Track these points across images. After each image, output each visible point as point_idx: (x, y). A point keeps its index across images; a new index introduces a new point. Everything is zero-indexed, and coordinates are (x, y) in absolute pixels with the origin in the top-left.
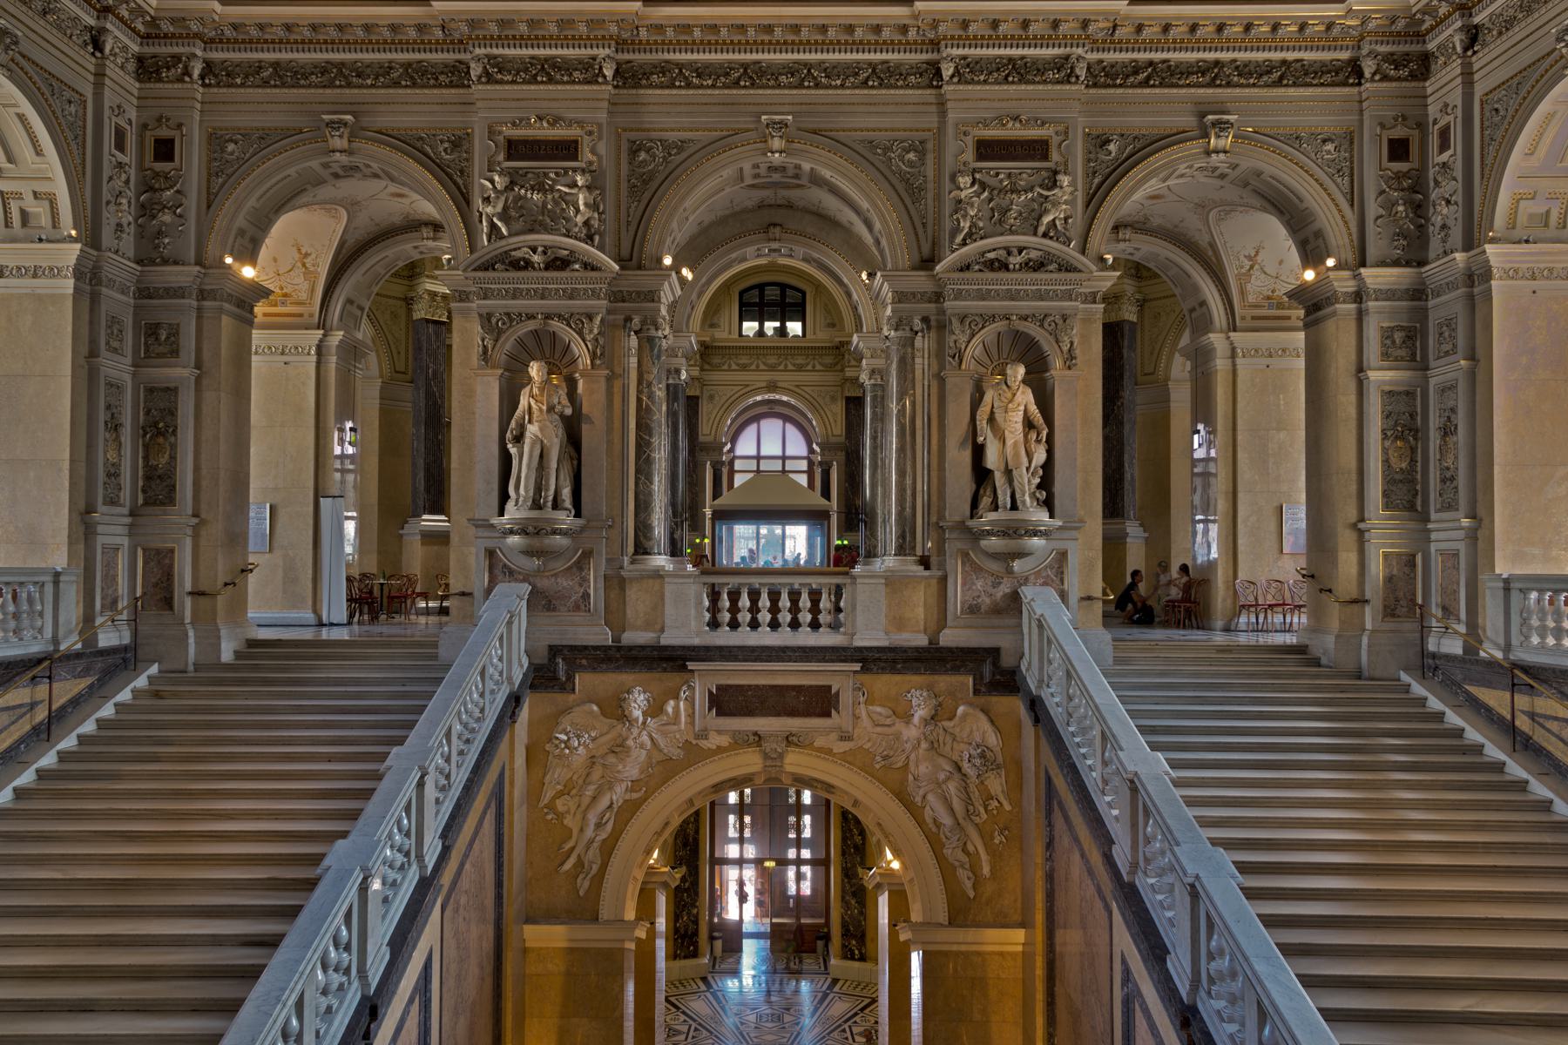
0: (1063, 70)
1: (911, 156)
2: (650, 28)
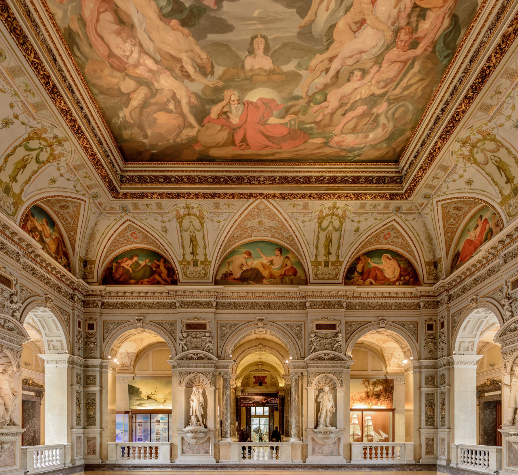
0: (339, 305)
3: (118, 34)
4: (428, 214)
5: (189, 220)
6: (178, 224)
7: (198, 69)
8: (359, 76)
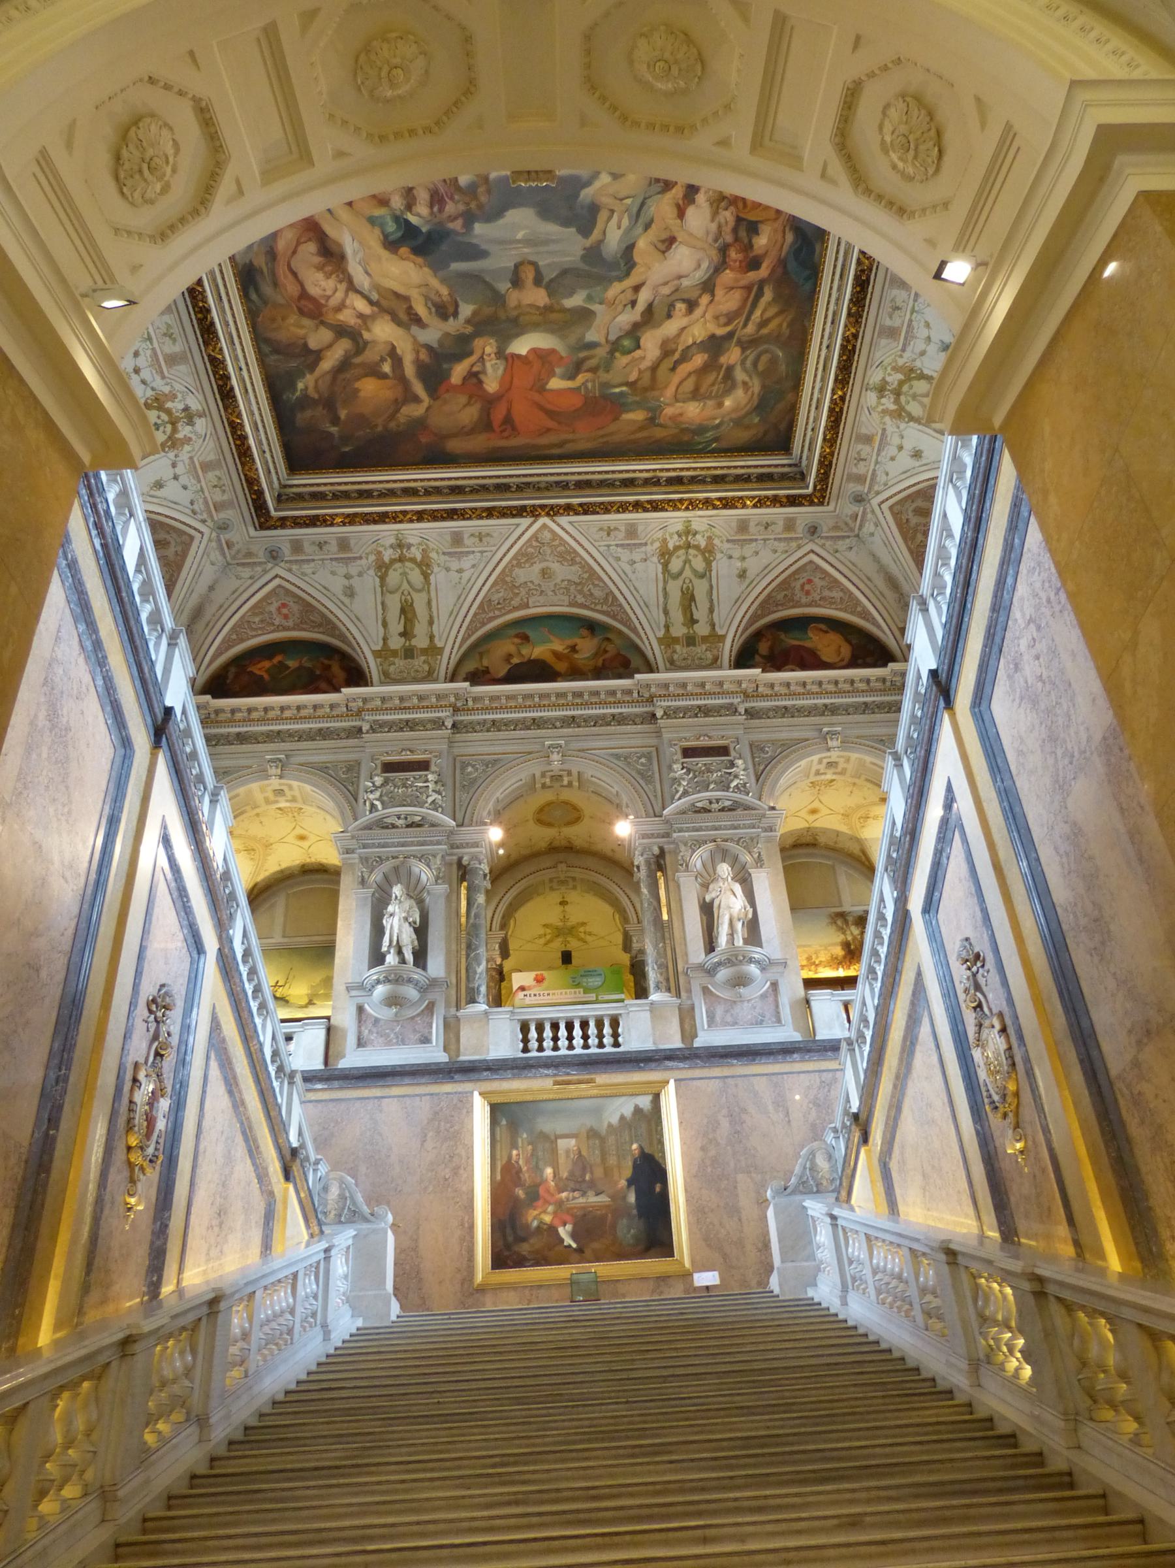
1: (643, 760)
3: (320, 268)
4: (872, 534)
5: (400, 571)
6: (377, 580)
7: (433, 310)
8: (684, 310)
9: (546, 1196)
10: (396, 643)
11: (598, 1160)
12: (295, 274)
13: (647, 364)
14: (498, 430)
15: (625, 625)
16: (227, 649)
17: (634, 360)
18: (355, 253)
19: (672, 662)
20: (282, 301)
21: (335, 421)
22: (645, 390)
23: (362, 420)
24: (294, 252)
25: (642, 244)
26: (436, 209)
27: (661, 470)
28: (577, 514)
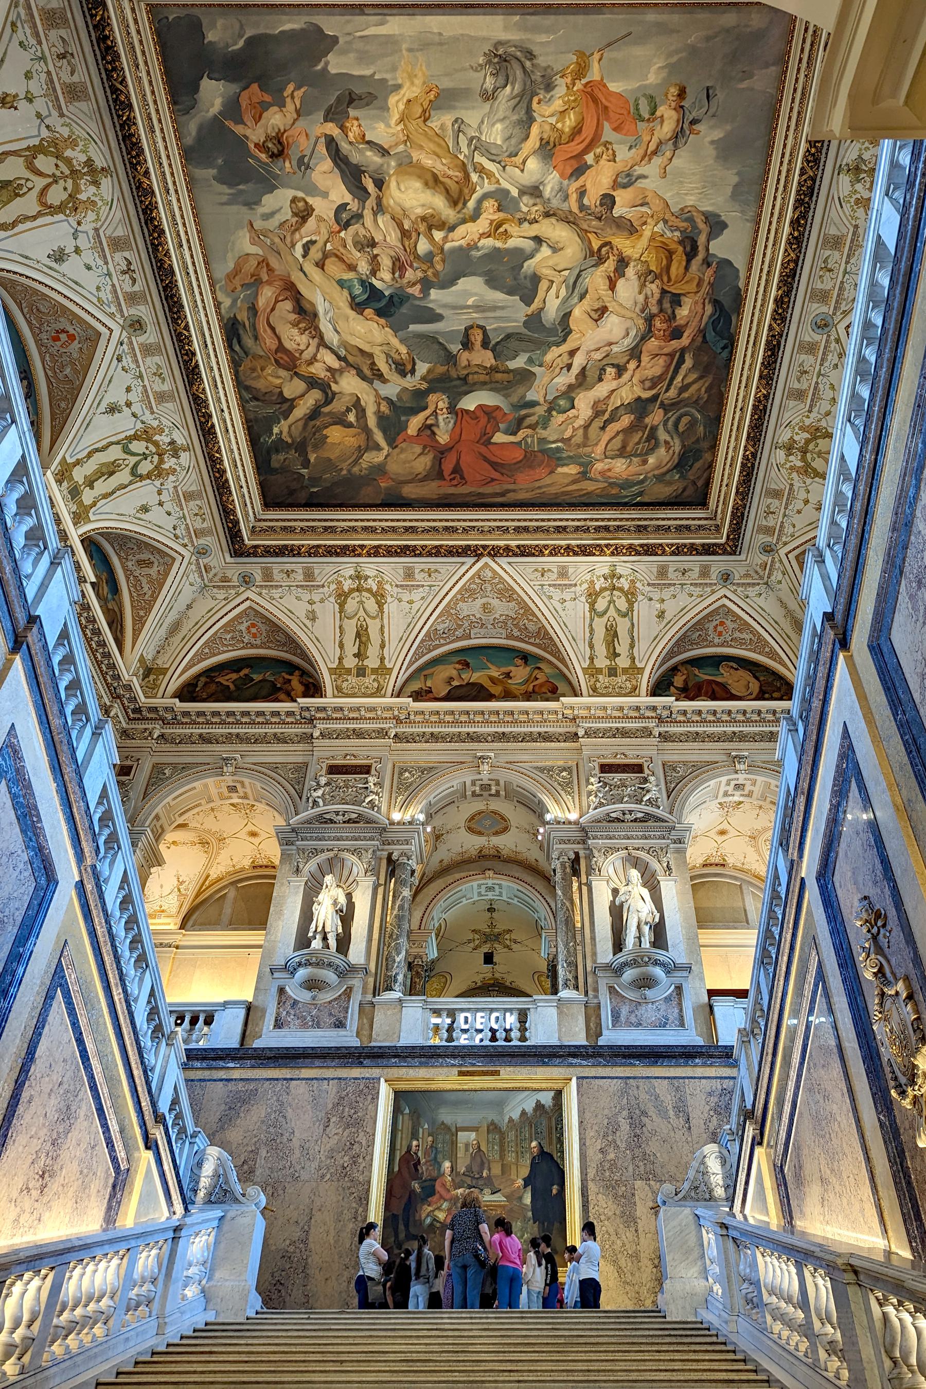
1: (564, 774)
2: (416, 713)
3: (295, 324)
5: (358, 599)
6: (337, 606)
7: (393, 366)
9: (443, 1193)
10: (350, 662)
11: (497, 1157)
12: (273, 329)
13: (580, 422)
14: (448, 478)
15: (554, 656)
16: (199, 662)
17: (568, 418)
18: (326, 313)
19: (595, 690)
20: (262, 353)
21: (306, 463)
22: (579, 446)
23: (329, 464)
24: (273, 309)
25: (577, 312)
26: (397, 275)
27: (591, 520)
28: (516, 555)
